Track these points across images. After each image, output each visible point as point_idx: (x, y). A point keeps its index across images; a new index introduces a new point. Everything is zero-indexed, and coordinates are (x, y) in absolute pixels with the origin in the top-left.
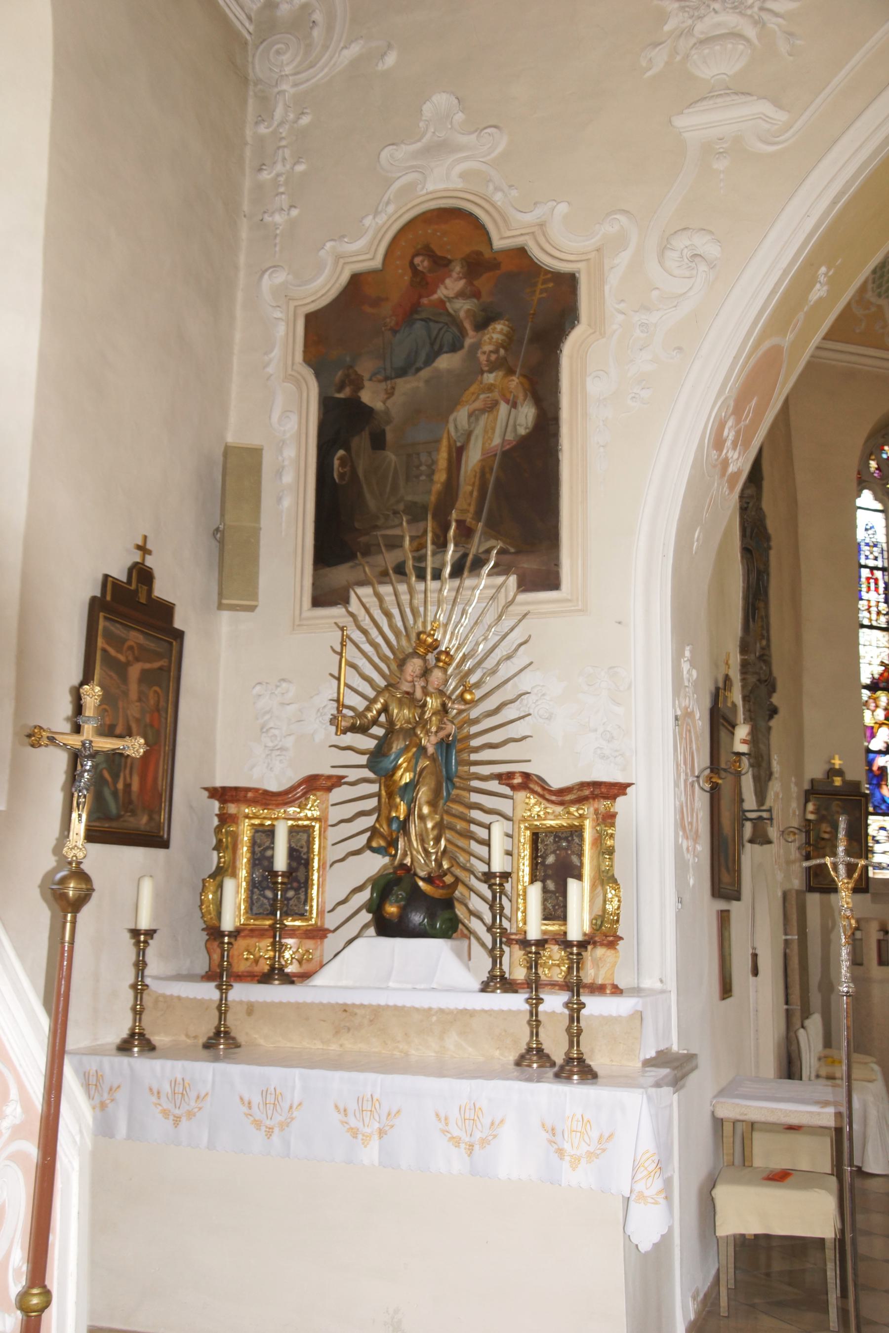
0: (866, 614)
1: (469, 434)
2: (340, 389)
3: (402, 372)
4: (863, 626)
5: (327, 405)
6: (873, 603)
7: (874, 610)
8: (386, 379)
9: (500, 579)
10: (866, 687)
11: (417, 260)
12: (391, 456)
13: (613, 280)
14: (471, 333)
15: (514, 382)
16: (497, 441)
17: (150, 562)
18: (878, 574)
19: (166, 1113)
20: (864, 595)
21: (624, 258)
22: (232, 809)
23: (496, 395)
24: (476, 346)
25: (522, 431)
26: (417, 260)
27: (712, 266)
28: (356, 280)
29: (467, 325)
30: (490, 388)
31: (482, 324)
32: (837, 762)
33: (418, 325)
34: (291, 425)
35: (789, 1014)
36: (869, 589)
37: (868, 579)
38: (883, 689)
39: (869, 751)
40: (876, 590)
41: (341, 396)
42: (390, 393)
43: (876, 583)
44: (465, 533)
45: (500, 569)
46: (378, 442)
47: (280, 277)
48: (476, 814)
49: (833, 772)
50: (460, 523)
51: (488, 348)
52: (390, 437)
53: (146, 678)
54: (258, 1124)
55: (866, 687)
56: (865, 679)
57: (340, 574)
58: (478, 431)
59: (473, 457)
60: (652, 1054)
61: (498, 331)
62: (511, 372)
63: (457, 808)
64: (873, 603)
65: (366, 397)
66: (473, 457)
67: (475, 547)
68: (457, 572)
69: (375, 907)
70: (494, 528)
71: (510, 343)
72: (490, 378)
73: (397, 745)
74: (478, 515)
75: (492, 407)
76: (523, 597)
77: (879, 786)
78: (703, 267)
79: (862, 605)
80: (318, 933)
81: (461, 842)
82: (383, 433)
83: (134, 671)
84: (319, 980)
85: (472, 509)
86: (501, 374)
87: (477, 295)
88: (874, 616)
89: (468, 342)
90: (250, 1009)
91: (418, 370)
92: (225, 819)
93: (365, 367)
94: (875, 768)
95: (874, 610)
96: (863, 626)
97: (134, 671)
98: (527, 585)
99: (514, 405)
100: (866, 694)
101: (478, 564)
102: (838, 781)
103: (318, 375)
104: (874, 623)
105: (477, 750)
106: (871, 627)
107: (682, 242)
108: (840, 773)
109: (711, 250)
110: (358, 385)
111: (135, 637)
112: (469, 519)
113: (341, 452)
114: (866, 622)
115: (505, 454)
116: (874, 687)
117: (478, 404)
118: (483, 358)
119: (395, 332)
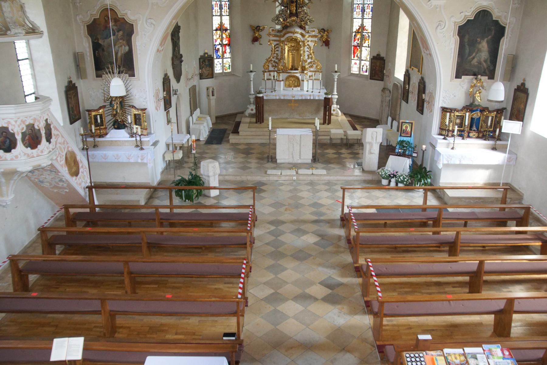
0: (215, 13)
1: (118, 51)
2: (95, 40)
3: (106, 38)
4: (214, 16)
5: (93, 42)
6: (216, 10)
7: (217, 11)
8: (103, 39)
9: (126, 75)
10: (215, 30)
11: (106, 18)
12: (106, 53)
13: (139, 26)
14: (117, 33)
15: (125, 42)
16: (123, 52)
17: (71, 79)
18: (218, 2)
19: (92, 158)
20: (214, 8)
21: (141, 22)
22: (90, 113)
23: (122, 44)
24: (118, 35)
25: (127, 51)
26: (106, 18)
27: (154, 25)
28: (95, 20)
29: (116, 31)
30: (121, 43)
31: (118, 32)
32: (206, 51)
33: (107, 30)
34: (87, 45)
35: (191, 112)
36: (215, 6)
37: (215, 4)
38: (218, 30)
39: (215, 45)
40: (217, 6)
41: (95, 41)
42: (104, 42)
43: (217, 5)
44: (119, 67)
45: (126, 73)
46: (103, 50)
47: (81, 16)
48: (126, 110)
49: (205, 53)
50: (118, 65)
51: (120, 36)
52: (105, 49)
53: (74, 96)
54: (104, 158)
55: (215, 30)
56: (214, 28)
57: (100, 72)
58: (120, 50)
59: (119, 55)
60: (152, 144)
61: (121, 33)
62: (124, 40)
63: (123, 109)
64: (216, 10)
65: (100, 42)
66: (119, 55)
67: (121, 69)
68: (119, 73)
69: (114, 125)
70: (124, 67)
71: (123, 35)
72: (121, 41)
73: (113, 103)
74: (121, 64)
75: (121, 46)
76: (130, 78)
77: (217, 52)
78: (153, 26)
79: (214, 11)
80: (106, 128)
81: (125, 114)
82: (104, 49)
83: (72, 97)
84: (108, 136)
85: (120, 63)
86: (122, 41)
87: (116, 26)
88: (217, 13)
89: (116, 34)
90: (98, 141)
91: (108, 38)
92: (89, 114)
93: (99, 37)
94: (216, 49)
95: (217, 11)
96: (214, 16)
97: (72, 97)
98: (129, 76)
99: (125, 46)
100: (214, 32)
101: (122, 72)
102: (206, 55)
103: (91, 37)
104: (217, 15)
105: (125, 101)
106: (216, 16)
107: (149, 21)
108: (207, 53)
109: (154, 23)
110: (98, 40)
111: (72, 91)
112: (120, 64)
113: (97, 52)
114: (215, 15)
115: (125, 54)
116: (216, 30)
117: (119, 46)
118: (119, 37)
119: (103, 31)
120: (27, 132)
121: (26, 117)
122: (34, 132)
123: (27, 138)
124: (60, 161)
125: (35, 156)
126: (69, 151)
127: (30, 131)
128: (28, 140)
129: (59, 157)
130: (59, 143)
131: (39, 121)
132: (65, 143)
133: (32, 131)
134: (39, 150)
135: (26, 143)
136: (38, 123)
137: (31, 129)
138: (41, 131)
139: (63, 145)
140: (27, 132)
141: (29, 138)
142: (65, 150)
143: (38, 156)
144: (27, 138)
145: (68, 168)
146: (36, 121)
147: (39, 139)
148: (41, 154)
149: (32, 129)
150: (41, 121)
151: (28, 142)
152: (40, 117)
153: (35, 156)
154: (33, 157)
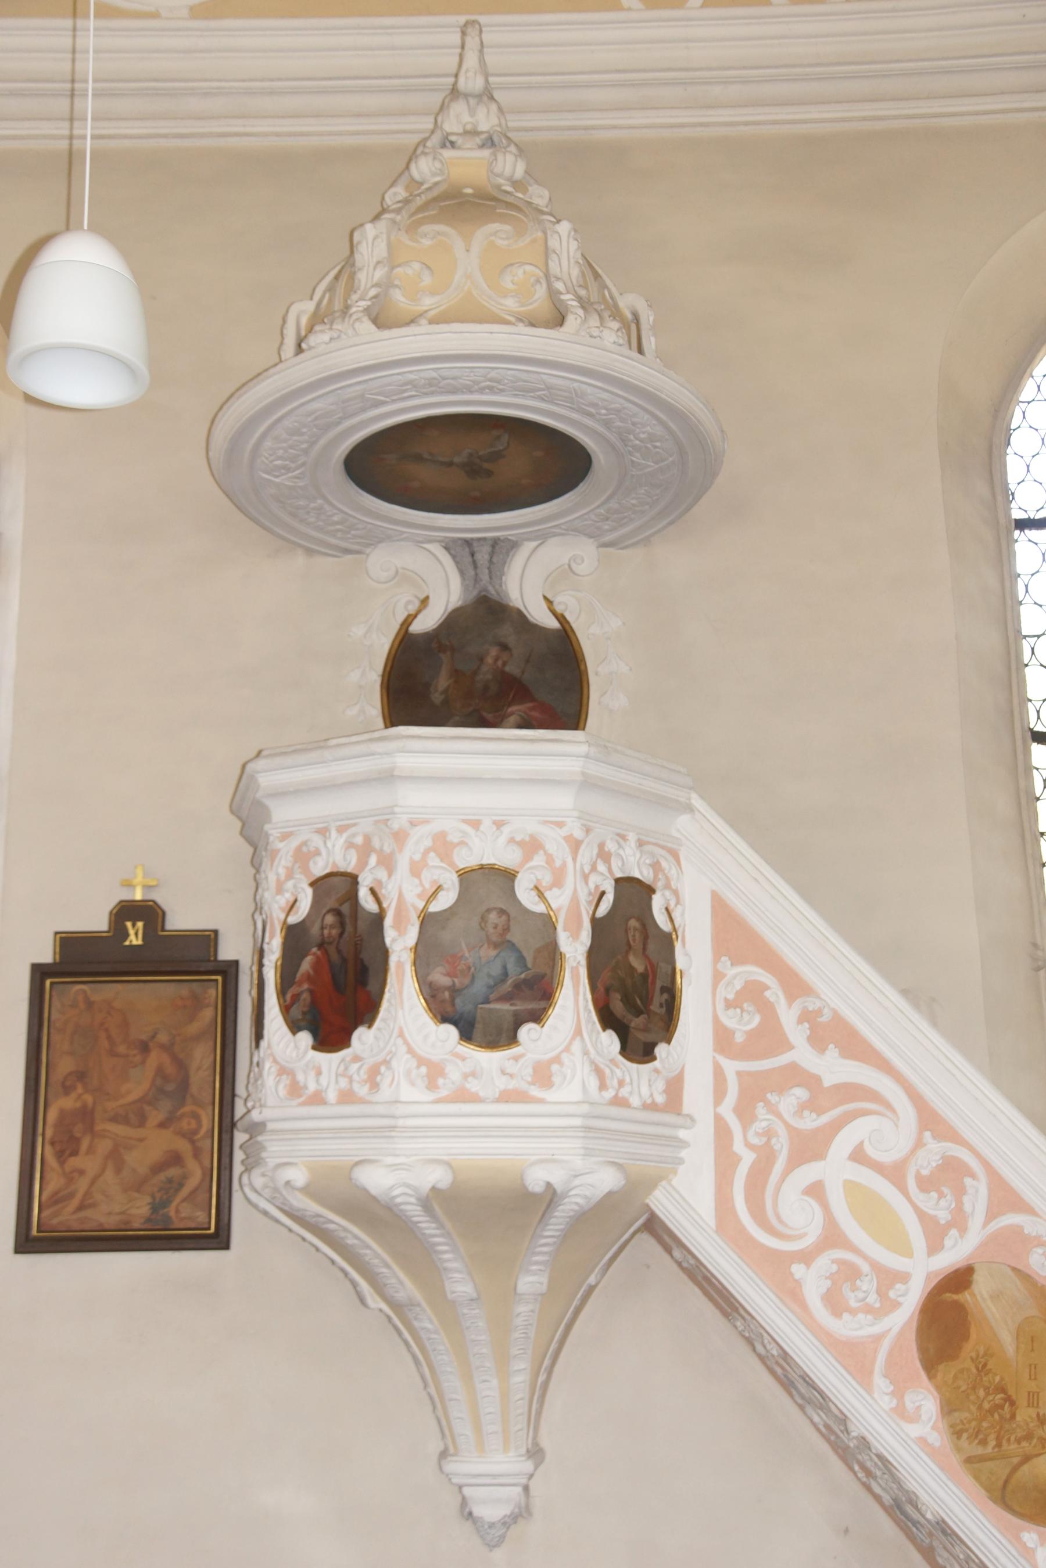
120: (315, 930)
121: (323, 832)
122: (349, 928)
123: (306, 965)
124: (834, 1303)
125: (331, 1096)
126: (1025, 1277)
127: (330, 919)
128: (308, 978)
129: (824, 1263)
130: (858, 1156)
131: (388, 863)
132: (960, 1191)
133: (342, 924)
134: (357, 1059)
135: (296, 998)
136: (382, 874)
137: (338, 913)
138: (390, 935)
139: (927, 1202)
140: (315, 930)
141: (316, 966)
142: (935, 1247)
143: (347, 1097)
144: (306, 965)
145: (948, 1408)
146: (373, 860)
147: (372, 986)
148: (362, 1091)
149: (345, 909)
150: (403, 863)
151: (306, 996)
152: (400, 837)
153: (331, 1096)
154: (317, 1099)
